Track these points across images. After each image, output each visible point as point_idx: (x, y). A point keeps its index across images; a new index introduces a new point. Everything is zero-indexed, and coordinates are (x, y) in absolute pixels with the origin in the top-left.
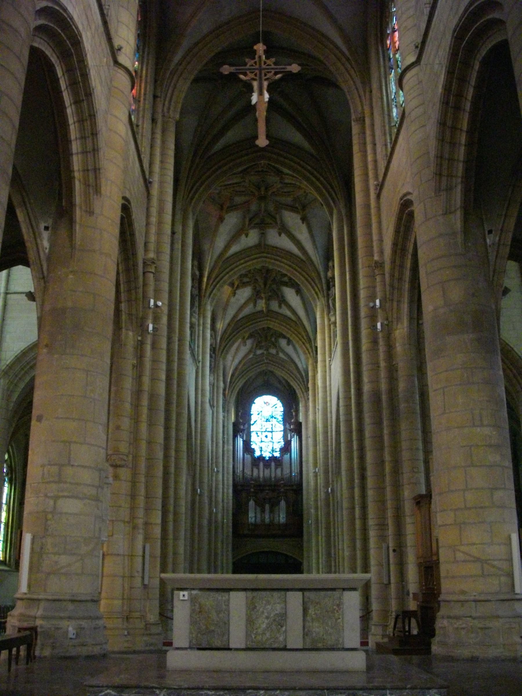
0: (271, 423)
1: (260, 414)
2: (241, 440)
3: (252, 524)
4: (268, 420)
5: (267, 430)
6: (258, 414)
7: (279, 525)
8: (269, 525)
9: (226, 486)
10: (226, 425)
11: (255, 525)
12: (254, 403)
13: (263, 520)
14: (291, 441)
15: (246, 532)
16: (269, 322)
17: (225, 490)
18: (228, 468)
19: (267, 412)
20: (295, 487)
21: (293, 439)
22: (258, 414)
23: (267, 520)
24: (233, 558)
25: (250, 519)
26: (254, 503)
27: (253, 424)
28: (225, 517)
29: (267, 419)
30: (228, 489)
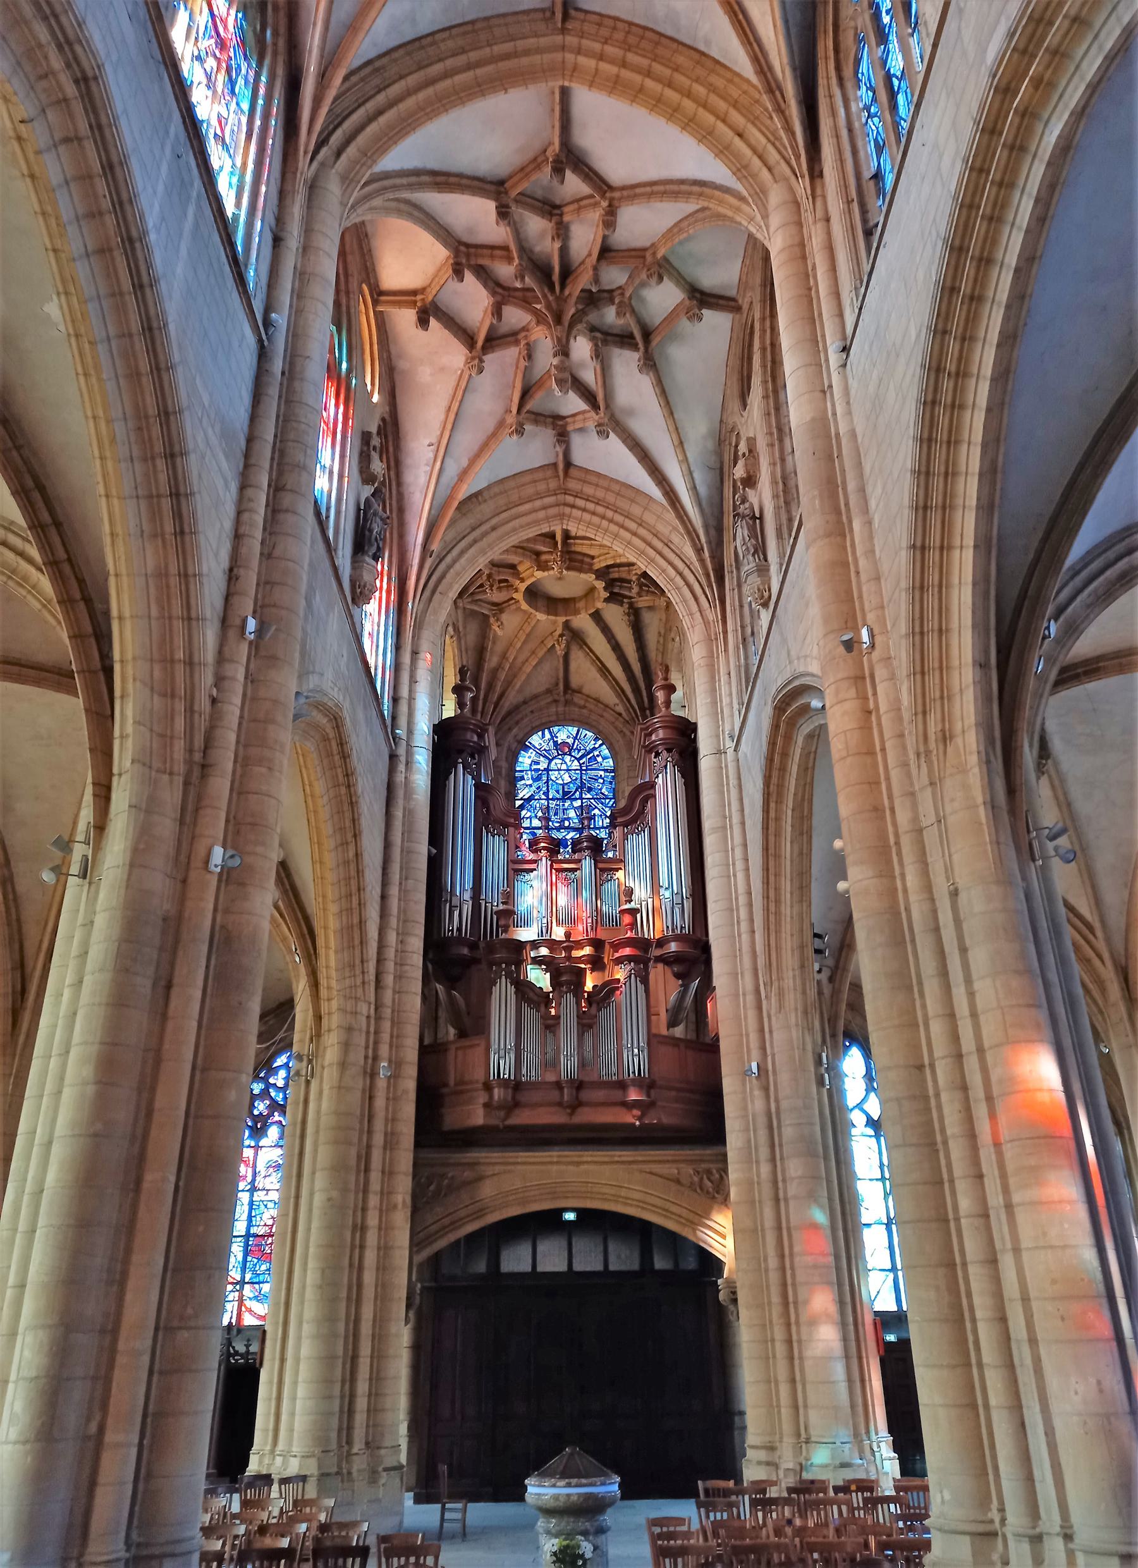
0: (577, 803)
1: (544, 778)
2: (470, 782)
3: (505, 1083)
4: (566, 795)
5: (567, 824)
6: (538, 779)
7: (622, 1085)
8: (579, 1086)
9: (393, 922)
10: (404, 692)
11: (516, 1086)
12: (526, 748)
13: (551, 1064)
14: (652, 785)
15: (478, 1117)
16: (570, 57)
17: (392, 938)
18: (407, 853)
19: (564, 771)
20: (673, 947)
21: (660, 781)
22: (538, 779)
23: (568, 1064)
24: (416, 1244)
25: (494, 1058)
26: (512, 990)
27: (522, 807)
28: (384, 1050)
29: (565, 793)
30: (403, 936)
